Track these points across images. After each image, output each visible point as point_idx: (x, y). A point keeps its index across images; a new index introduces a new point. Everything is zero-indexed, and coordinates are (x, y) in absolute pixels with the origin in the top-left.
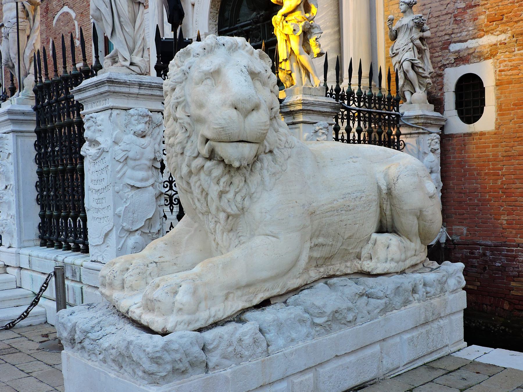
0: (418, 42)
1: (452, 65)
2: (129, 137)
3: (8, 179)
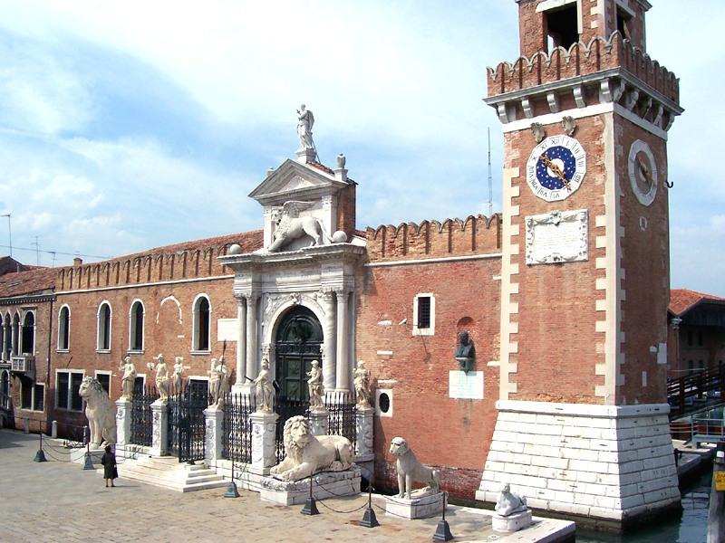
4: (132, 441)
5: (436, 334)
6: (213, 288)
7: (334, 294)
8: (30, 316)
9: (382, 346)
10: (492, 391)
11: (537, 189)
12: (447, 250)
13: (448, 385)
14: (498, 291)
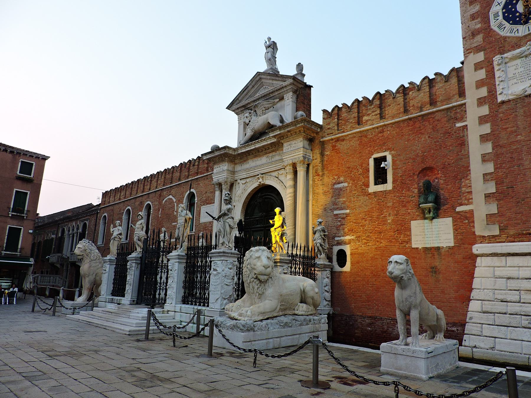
0: (323, 236)
1: (335, 245)
2: (227, 269)
3: (174, 279)
4: (113, 294)
5: (394, 187)
6: (199, 184)
7: (294, 166)
8: (85, 225)
9: (338, 206)
10: (465, 235)
11: (507, 30)
12: (402, 110)
13: (410, 235)
14: (464, 136)
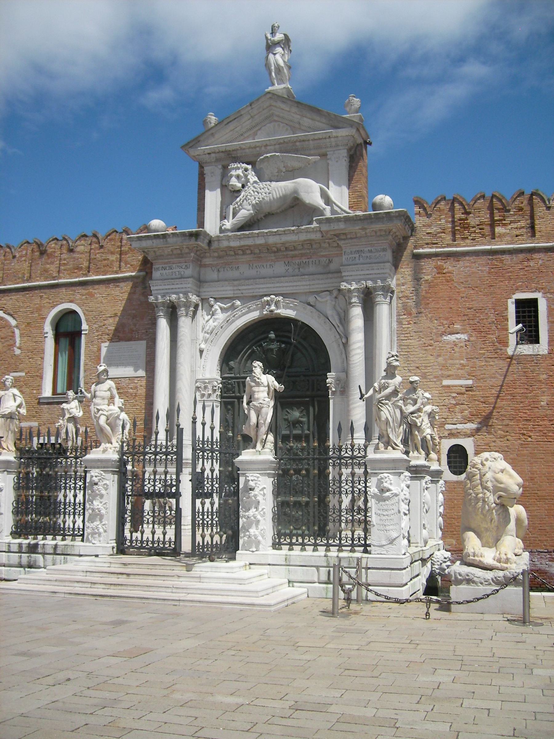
1: (445, 437)
4: (16, 534)
6: (91, 295)
9: (450, 373)
